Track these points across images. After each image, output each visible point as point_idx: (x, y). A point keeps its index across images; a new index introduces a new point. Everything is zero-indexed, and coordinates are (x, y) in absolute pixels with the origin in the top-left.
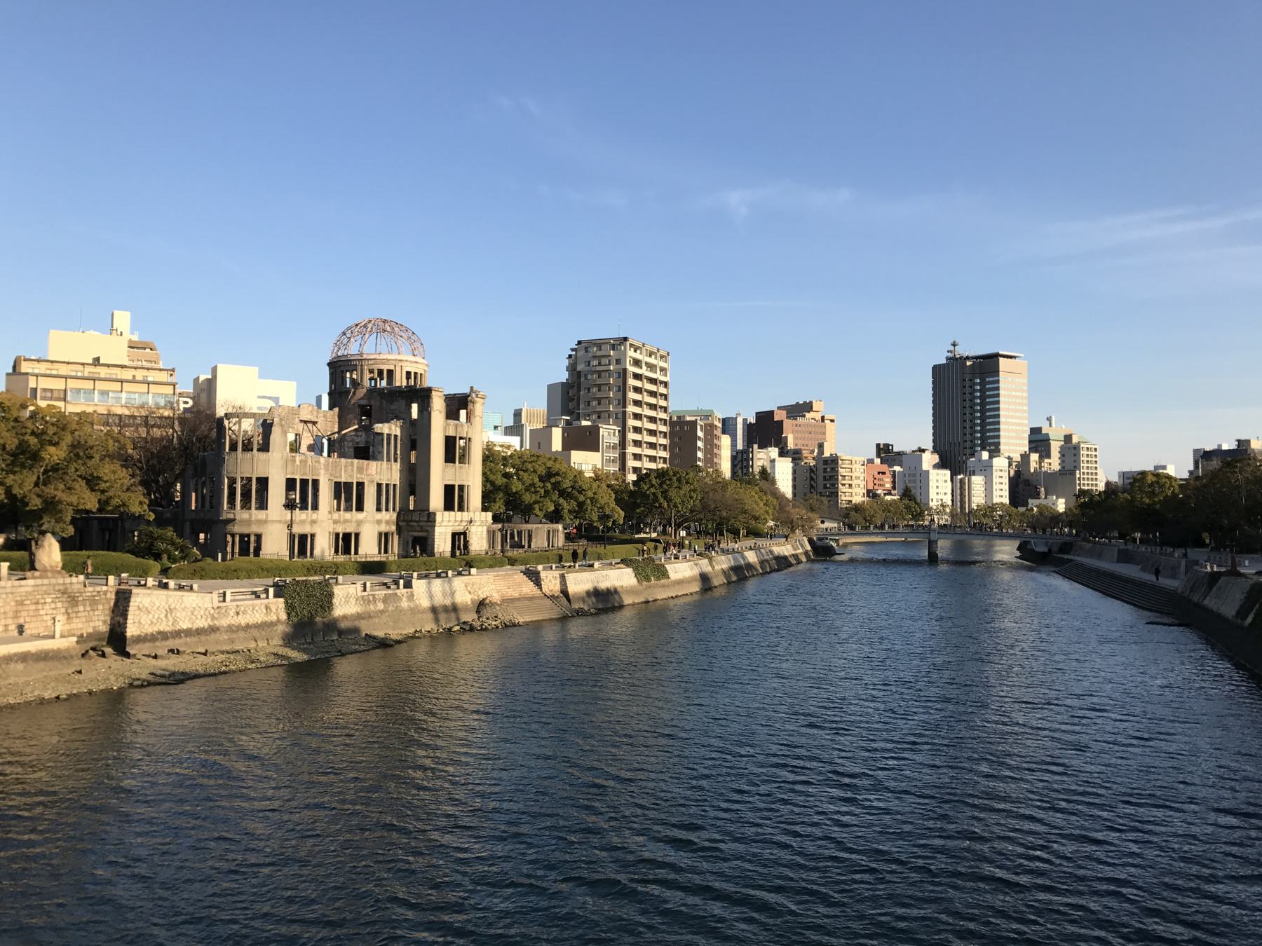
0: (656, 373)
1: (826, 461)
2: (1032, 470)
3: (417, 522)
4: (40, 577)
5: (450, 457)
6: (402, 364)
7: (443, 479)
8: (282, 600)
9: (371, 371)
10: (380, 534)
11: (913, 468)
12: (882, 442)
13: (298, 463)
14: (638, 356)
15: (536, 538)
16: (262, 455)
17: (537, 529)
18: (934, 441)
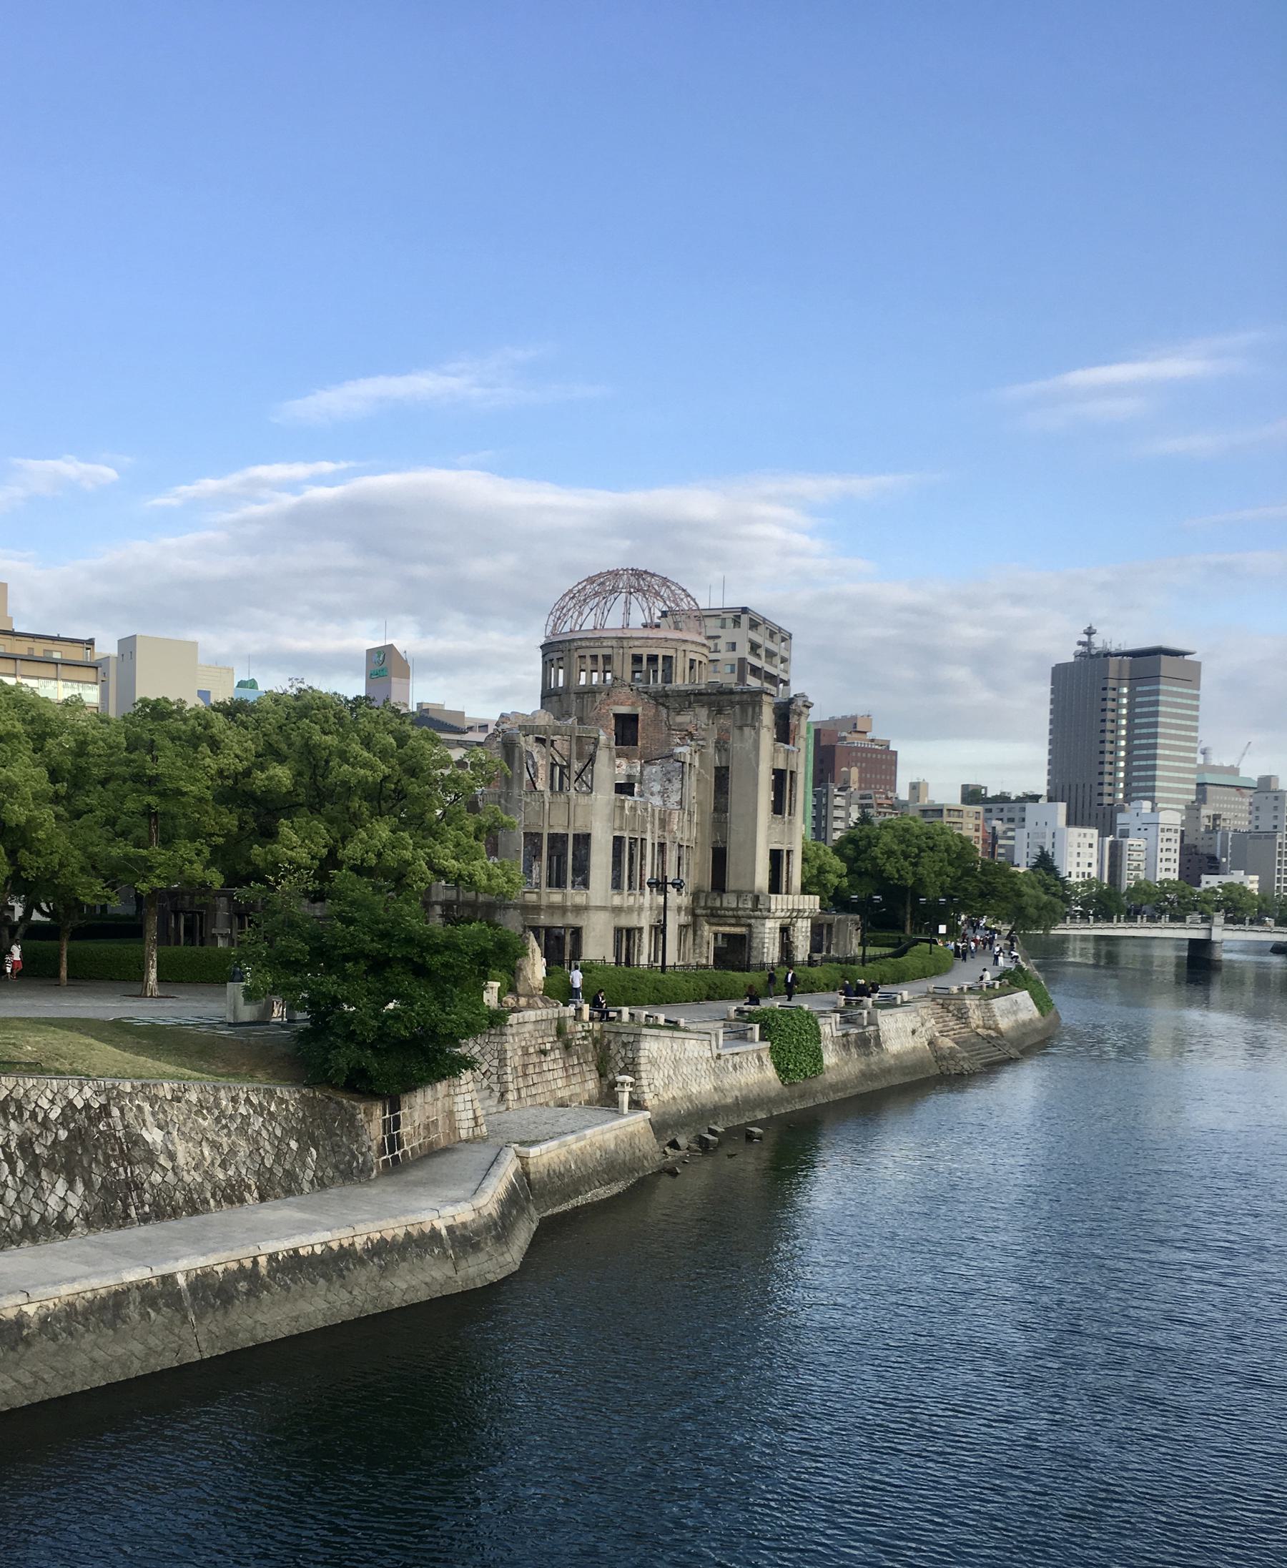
0: (776, 667)
1: (924, 812)
2: (1203, 829)
3: (733, 909)
4: (529, 1006)
5: (778, 808)
6: (689, 647)
7: (768, 842)
8: (768, 1044)
9: (637, 659)
10: (680, 926)
11: (1042, 824)
12: (972, 781)
13: (627, 812)
14: (754, 636)
15: (837, 937)
16: (583, 800)
17: (839, 921)
18: (1049, 782)
